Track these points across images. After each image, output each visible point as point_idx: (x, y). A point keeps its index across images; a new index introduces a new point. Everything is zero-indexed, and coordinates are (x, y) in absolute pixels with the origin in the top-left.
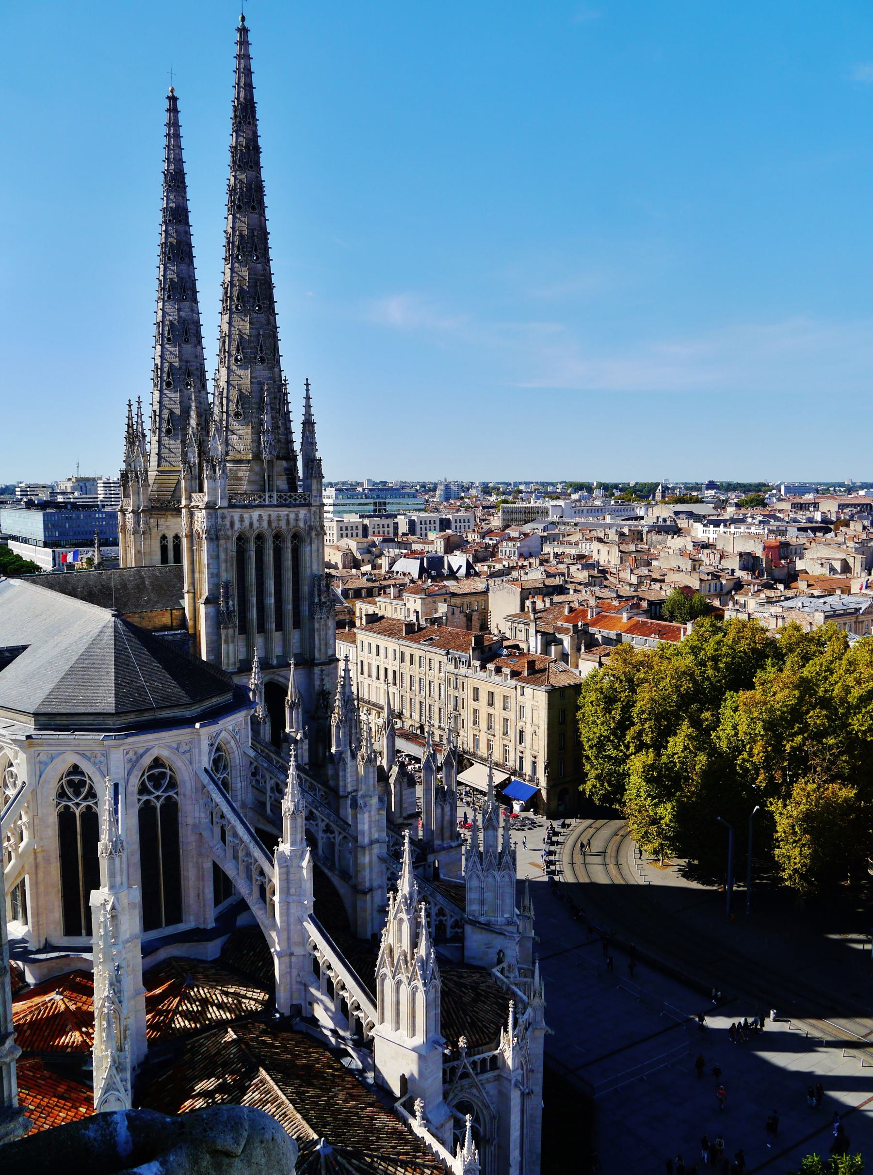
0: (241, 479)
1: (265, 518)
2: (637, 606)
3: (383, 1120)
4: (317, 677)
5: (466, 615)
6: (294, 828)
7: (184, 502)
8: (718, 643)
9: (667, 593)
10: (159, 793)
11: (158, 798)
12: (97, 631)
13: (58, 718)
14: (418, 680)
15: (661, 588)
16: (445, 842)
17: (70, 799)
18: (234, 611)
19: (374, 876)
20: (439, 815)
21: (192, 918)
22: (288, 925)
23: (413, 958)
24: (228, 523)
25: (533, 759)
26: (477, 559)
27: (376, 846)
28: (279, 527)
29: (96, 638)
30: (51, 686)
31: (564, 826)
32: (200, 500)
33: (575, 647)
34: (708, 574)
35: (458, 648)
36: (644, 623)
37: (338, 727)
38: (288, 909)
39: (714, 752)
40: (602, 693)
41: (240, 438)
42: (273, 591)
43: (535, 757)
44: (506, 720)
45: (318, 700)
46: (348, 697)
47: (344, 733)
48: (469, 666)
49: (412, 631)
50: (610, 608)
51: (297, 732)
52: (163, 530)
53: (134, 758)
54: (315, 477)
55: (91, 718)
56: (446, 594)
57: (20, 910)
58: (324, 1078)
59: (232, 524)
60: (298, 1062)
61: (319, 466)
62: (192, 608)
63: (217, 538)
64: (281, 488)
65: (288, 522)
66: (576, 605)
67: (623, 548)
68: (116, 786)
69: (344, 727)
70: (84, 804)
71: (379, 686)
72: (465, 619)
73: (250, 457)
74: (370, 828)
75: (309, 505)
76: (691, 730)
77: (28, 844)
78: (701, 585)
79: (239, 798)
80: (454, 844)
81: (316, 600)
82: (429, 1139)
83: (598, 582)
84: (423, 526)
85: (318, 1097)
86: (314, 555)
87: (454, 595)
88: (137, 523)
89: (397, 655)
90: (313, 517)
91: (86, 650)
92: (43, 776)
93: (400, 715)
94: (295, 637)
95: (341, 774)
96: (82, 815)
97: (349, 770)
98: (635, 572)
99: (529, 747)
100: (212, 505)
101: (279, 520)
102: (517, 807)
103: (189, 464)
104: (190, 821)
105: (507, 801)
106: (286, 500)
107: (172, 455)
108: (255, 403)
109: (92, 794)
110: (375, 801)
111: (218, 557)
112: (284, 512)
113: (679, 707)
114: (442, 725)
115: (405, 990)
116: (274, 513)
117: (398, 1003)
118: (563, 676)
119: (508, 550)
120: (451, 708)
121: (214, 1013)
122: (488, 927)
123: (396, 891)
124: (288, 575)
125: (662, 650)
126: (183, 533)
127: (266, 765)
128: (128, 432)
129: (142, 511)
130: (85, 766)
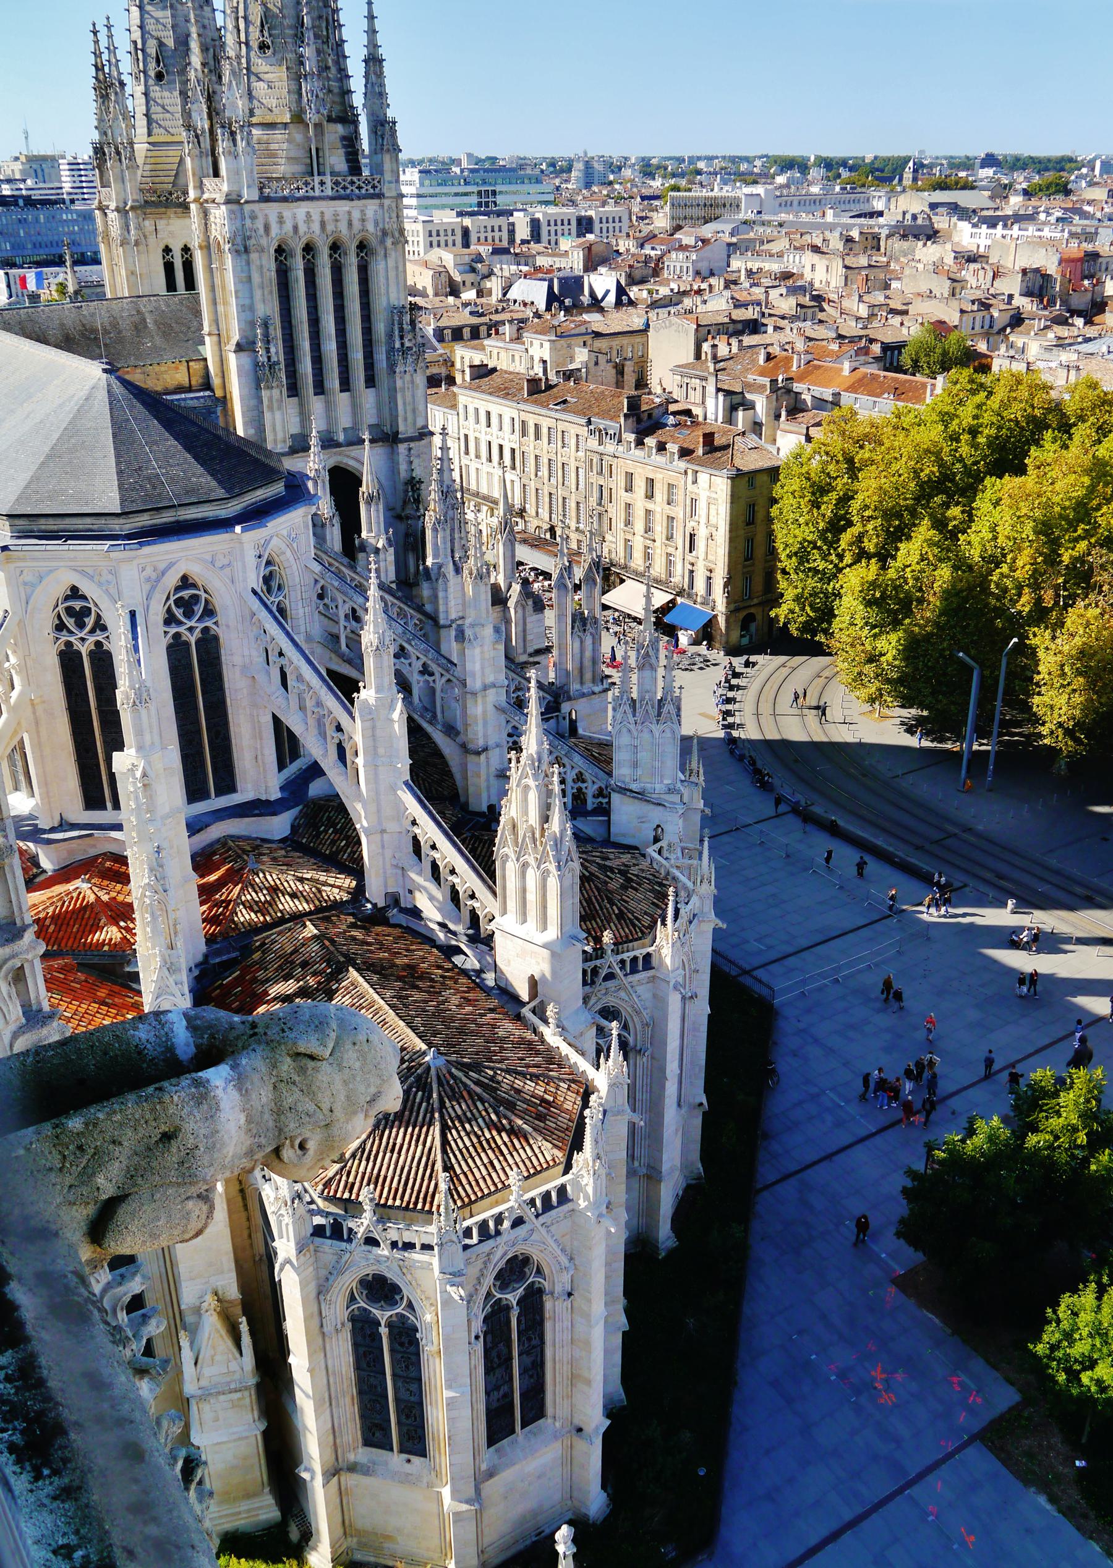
0: (274, 156)
1: (316, 217)
2: (865, 351)
3: (507, 1028)
5: (616, 366)
6: (379, 668)
7: (192, 194)
8: (979, 406)
9: (909, 331)
10: (190, 624)
11: (191, 629)
12: (83, 394)
13: (42, 521)
14: (546, 461)
15: (902, 324)
17: (70, 632)
18: (278, 363)
19: (490, 732)
20: (577, 650)
21: (249, 786)
22: (377, 793)
23: (542, 836)
24: (260, 225)
26: (633, 281)
27: (491, 692)
29: (82, 406)
30: (27, 476)
31: (747, 664)
32: (217, 189)
33: (772, 413)
34: (973, 302)
35: (604, 415)
36: (874, 377)
37: (435, 530)
38: (376, 774)
39: (961, 565)
40: (808, 479)
41: (270, 87)
44: (671, 519)
48: (620, 441)
49: (537, 388)
50: (826, 354)
51: (378, 537)
52: (165, 239)
53: (154, 576)
55: (88, 520)
57: (22, 778)
58: (432, 980)
59: (267, 228)
60: (398, 961)
61: (393, 132)
62: (217, 359)
63: (246, 250)
65: (350, 224)
66: (775, 350)
67: (850, 261)
68: (133, 614)
70: (92, 639)
71: (491, 470)
72: (614, 371)
73: (287, 118)
74: (483, 668)
75: (380, 196)
76: (933, 532)
77: (21, 694)
79: (303, 629)
80: (597, 689)
81: (397, 345)
82: (565, 1049)
83: (809, 316)
84: (553, 228)
85: (426, 1002)
86: (392, 274)
87: (598, 335)
88: (126, 227)
91: (70, 423)
92: (31, 602)
93: (522, 513)
95: (441, 594)
96: (91, 654)
97: (451, 590)
98: (866, 298)
99: (702, 556)
100: (234, 197)
102: (684, 639)
104: (237, 660)
105: (670, 631)
106: (344, 188)
107: (168, 115)
108: (290, 27)
109: (100, 626)
110: (488, 631)
111: (249, 279)
112: (343, 207)
113: (917, 499)
114: (581, 526)
115: (532, 876)
116: (330, 208)
117: (524, 890)
118: (754, 455)
120: (593, 501)
121: (287, 904)
122: (640, 796)
123: (519, 750)
125: (898, 416)
126: (195, 243)
128: (96, 78)
129: (132, 208)
130: (85, 588)
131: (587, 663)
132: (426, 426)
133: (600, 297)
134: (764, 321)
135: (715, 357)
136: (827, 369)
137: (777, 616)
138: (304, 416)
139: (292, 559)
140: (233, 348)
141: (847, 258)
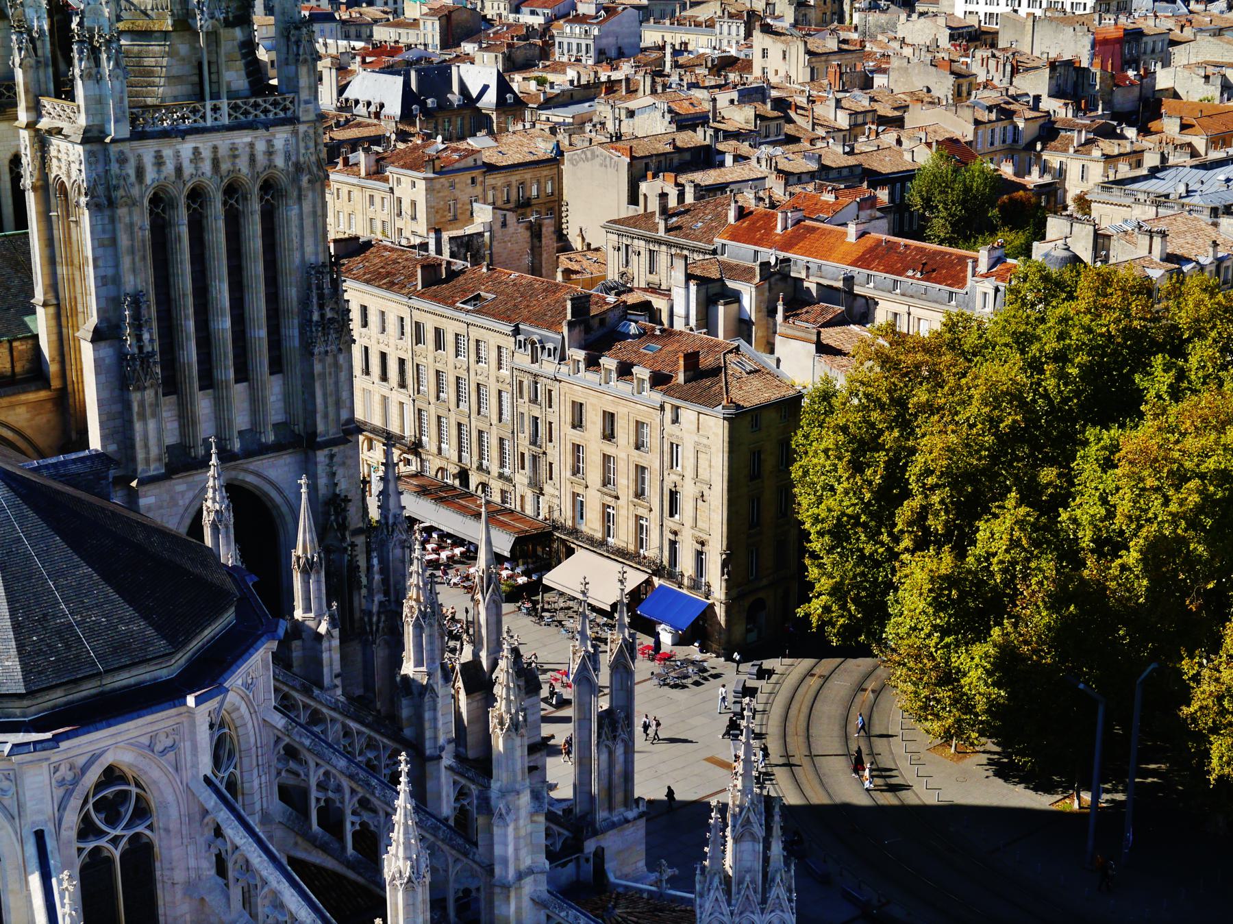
0: (150, 74)
1: (206, 153)
4: (321, 470)
6: (410, 906)
10: (118, 832)
11: (115, 841)
14: (452, 380)
15: (899, 142)
16: (615, 813)
20: (604, 765)
24: (131, 171)
25: (699, 547)
28: (235, 171)
31: (763, 674)
33: (764, 306)
34: (990, 109)
36: (892, 247)
37: (418, 627)
42: (227, 304)
43: (703, 544)
44: (641, 470)
45: (327, 514)
46: (395, 516)
47: (431, 636)
51: (319, 617)
53: (69, 776)
54: (305, 61)
56: (475, 167)
59: (140, 172)
62: (54, 337)
63: (112, 204)
64: (234, 86)
65: (252, 159)
68: (40, 836)
69: (431, 625)
71: (370, 387)
72: (528, 234)
73: (168, 24)
74: (516, 850)
75: (293, 121)
76: (1023, 510)
78: (976, 134)
79: (258, 807)
81: (316, 317)
83: (773, 129)
86: (308, 222)
87: (490, 168)
89: (408, 329)
90: (302, 145)
93: (416, 448)
94: (274, 389)
95: (427, 715)
97: (439, 705)
99: (689, 522)
100: (95, 133)
101: (235, 157)
102: (666, 638)
103: (30, 34)
104: (179, 876)
105: (649, 628)
106: (246, 113)
110: (525, 799)
111: (114, 241)
112: (243, 138)
113: (994, 459)
114: (507, 471)
116: (224, 141)
118: (756, 382)
119: (574, 42)
124: (256, 269)
127: (307, 742)
131: (617, 780)
132: (352, 419)
133: (474, 95)
134: (720, 147)
135: (665, 211)
136: (824, 233)
137: (807, 615)
138: (186, 419)
139: (247, 716)
140: (90, 336)
141: (810, 40)
